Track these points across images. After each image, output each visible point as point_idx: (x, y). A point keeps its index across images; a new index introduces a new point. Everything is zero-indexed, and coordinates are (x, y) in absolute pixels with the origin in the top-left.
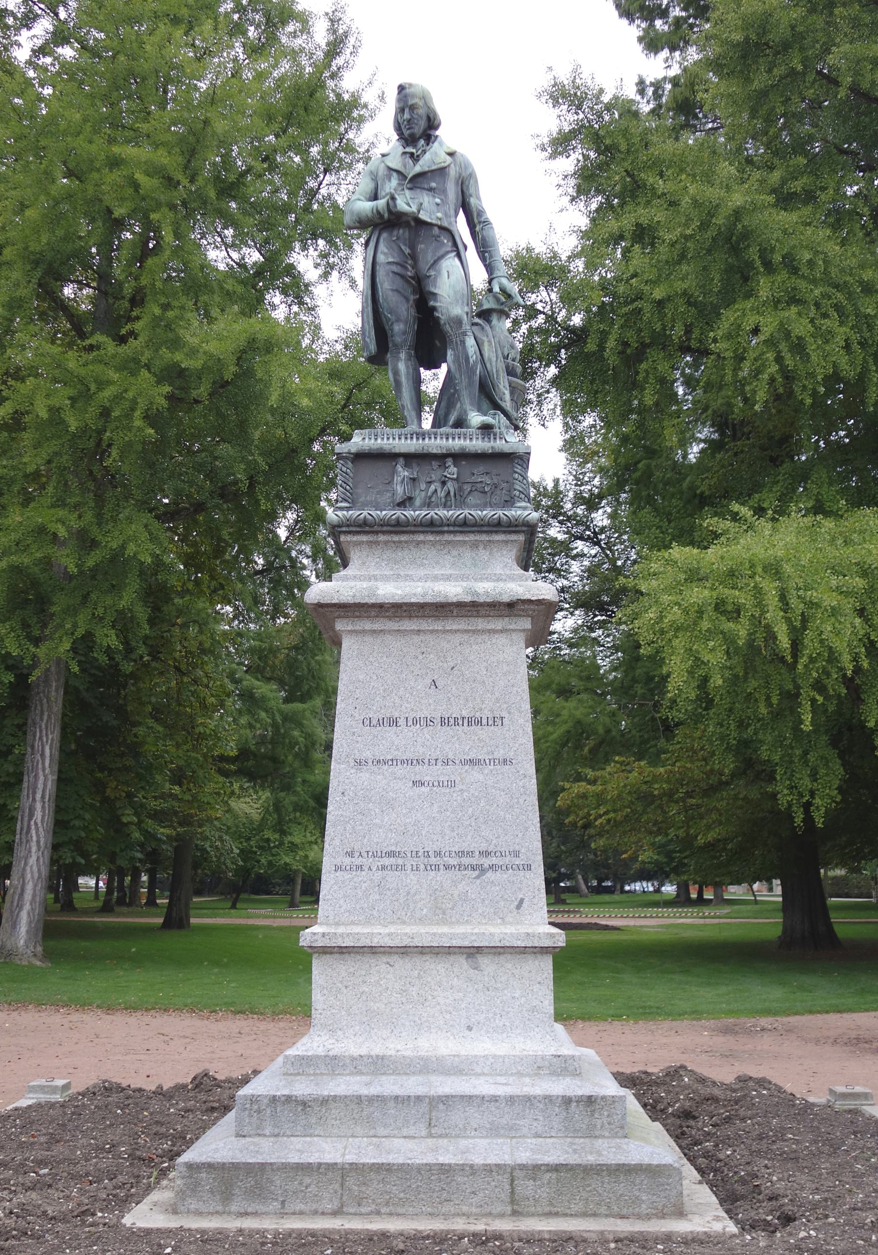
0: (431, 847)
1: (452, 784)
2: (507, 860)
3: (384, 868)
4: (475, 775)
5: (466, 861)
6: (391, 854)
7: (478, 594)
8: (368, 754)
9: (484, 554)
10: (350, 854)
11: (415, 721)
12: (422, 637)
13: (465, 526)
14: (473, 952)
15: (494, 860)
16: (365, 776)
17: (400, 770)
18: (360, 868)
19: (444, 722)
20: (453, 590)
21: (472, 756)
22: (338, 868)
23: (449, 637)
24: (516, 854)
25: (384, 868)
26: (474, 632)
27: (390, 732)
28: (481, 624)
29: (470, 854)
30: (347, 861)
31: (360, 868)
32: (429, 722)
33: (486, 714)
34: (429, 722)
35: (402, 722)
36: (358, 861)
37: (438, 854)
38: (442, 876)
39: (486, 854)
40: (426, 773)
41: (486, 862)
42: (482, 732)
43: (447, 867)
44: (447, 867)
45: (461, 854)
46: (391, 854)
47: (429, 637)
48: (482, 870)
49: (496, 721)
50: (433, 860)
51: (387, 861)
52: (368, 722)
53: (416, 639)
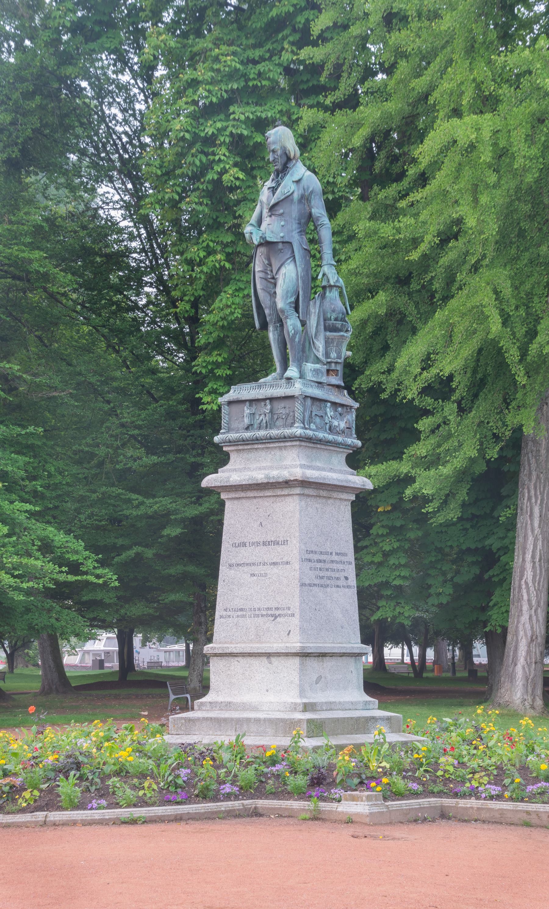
0: (257, 606)
1: (266, 575)
2: (285, 612)
3: (238, 616)
4: (276, 570)
5: (270, 612)
6: (241, 610)
7: (270, 478)
8: (234, 561)
9: (285, 453)
10: (226, 610)
11: (253, 544)
12: (257, 500)
13: (271, 439)
14: (268, 655)
15: (280, 612)
16: (233, 572)
17: (246, 569)
18: (229, 616)
19: (264, 544)
20: (260, 476)
21: (274, 561)
22: (221, 617)
23: (268, 499)
24: (289, 609)
25: (238, 616)
26: (278, 496)
27: (242, 550)
28: (279, 492)
29: (271, 609)
30: (225, 613)
31: (229, 616)
32: (258, 544)
33: (281, 539)
34: (258, 544)
35: (247, 544)
36: (229, 613)
37: (259, 609)
38: (260, 620)
39: (277, 609)
40: (257, 570)
41: (277, 613)
42: (279, 548)
43: (262, 616)
44: (262, 616)
45: (268, 609)
46: (241, 610)
47: (260, 500)
48: (276, 617)
49: (285, 542)
50: (257, 612)
51: (240, 613)
52: (234, 545)
53: (255, 501)
